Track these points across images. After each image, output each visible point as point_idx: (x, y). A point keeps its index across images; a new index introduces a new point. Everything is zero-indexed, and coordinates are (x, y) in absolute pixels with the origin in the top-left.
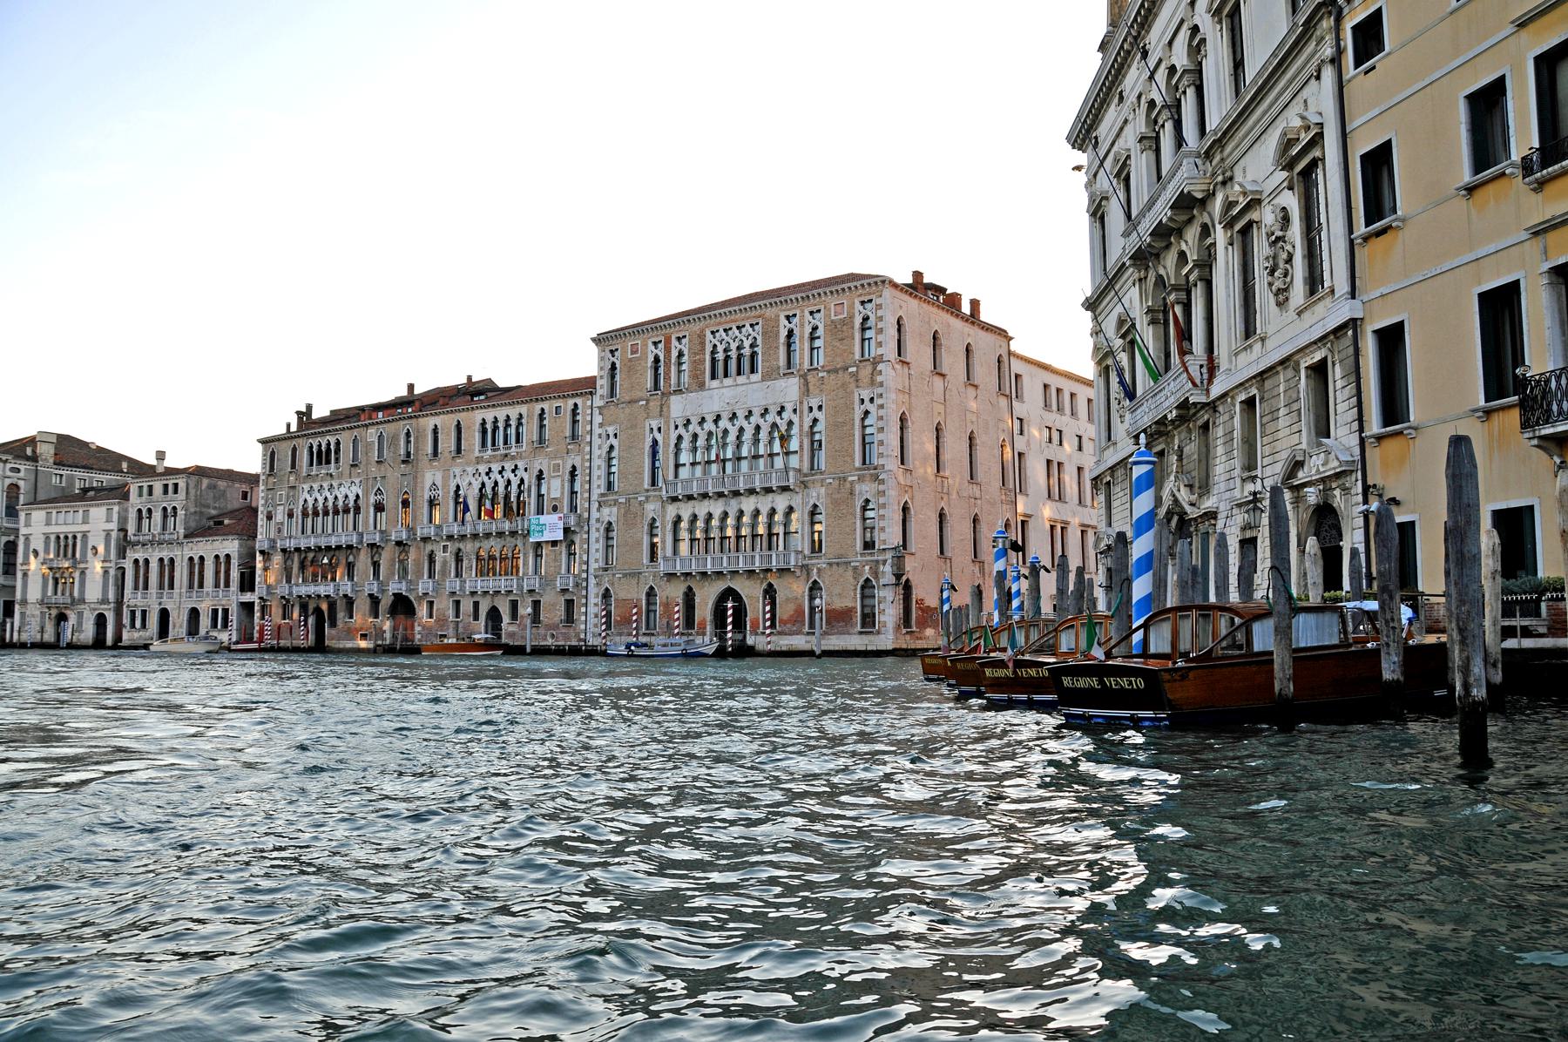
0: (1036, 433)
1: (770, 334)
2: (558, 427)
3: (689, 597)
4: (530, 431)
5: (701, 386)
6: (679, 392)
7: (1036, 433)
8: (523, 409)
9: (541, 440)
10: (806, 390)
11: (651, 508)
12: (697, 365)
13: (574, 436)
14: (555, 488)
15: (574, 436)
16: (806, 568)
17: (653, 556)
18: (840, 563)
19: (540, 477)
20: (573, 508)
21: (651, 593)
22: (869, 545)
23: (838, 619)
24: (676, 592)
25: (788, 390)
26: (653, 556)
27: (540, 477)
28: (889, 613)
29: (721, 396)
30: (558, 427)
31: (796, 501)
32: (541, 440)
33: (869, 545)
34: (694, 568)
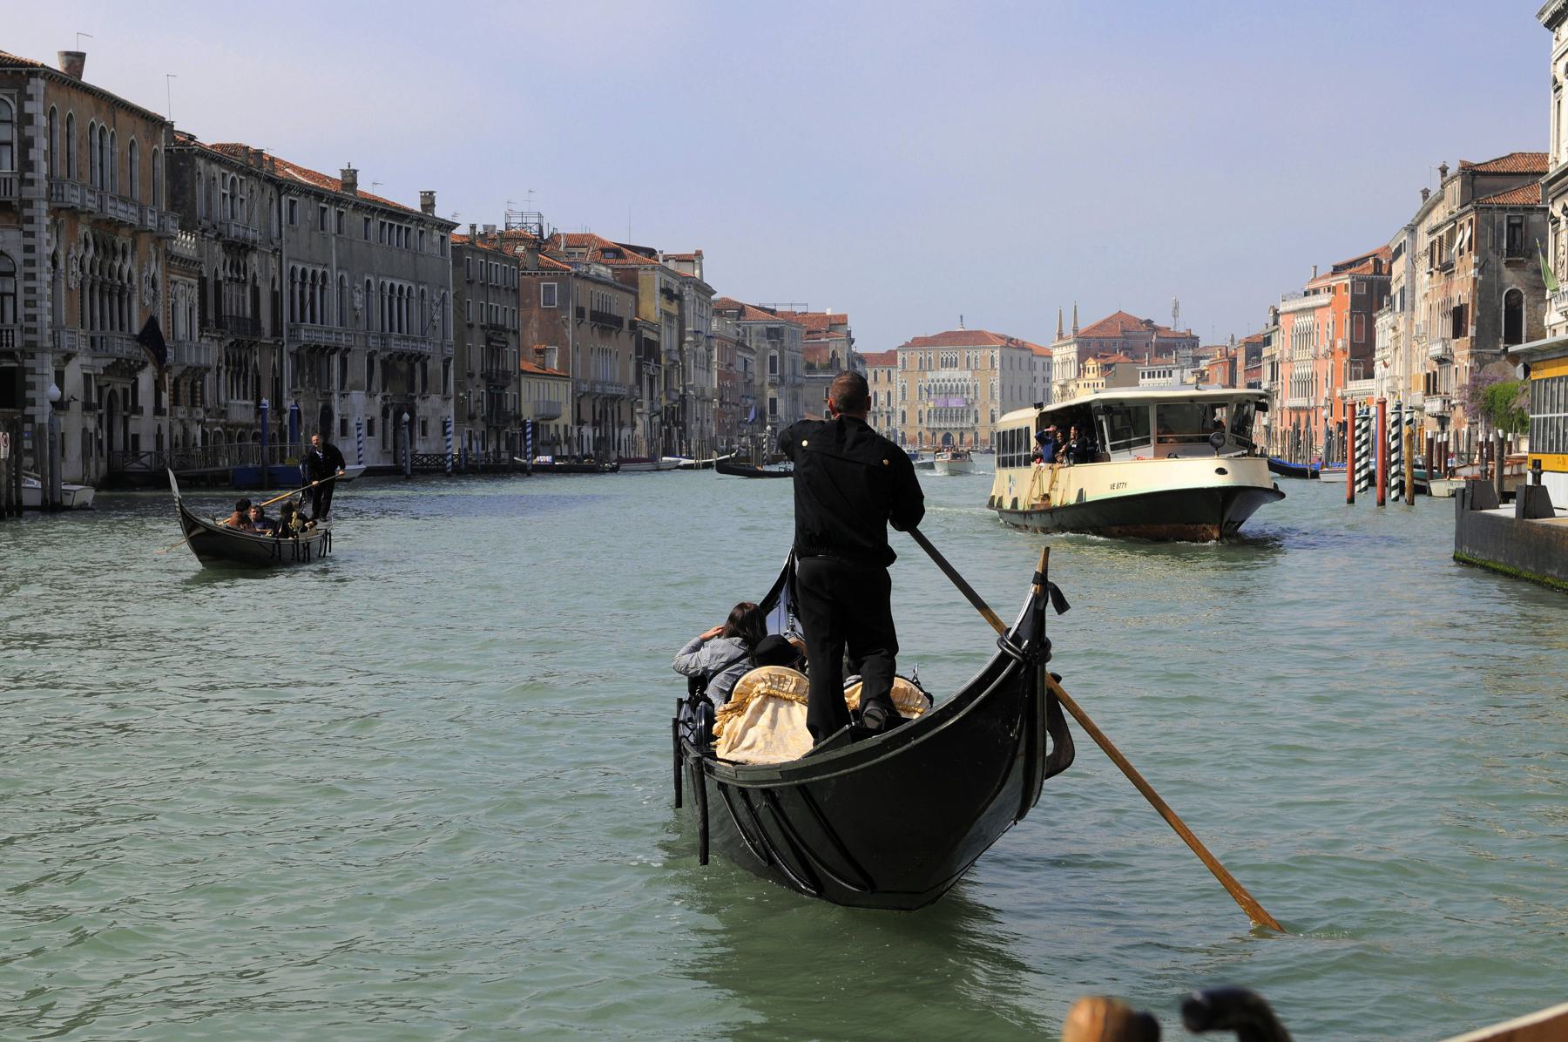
0: (1039, 380)
7: (1039, 380)
25: (969, 374)
29: (945, 373)
30: (882, 376)
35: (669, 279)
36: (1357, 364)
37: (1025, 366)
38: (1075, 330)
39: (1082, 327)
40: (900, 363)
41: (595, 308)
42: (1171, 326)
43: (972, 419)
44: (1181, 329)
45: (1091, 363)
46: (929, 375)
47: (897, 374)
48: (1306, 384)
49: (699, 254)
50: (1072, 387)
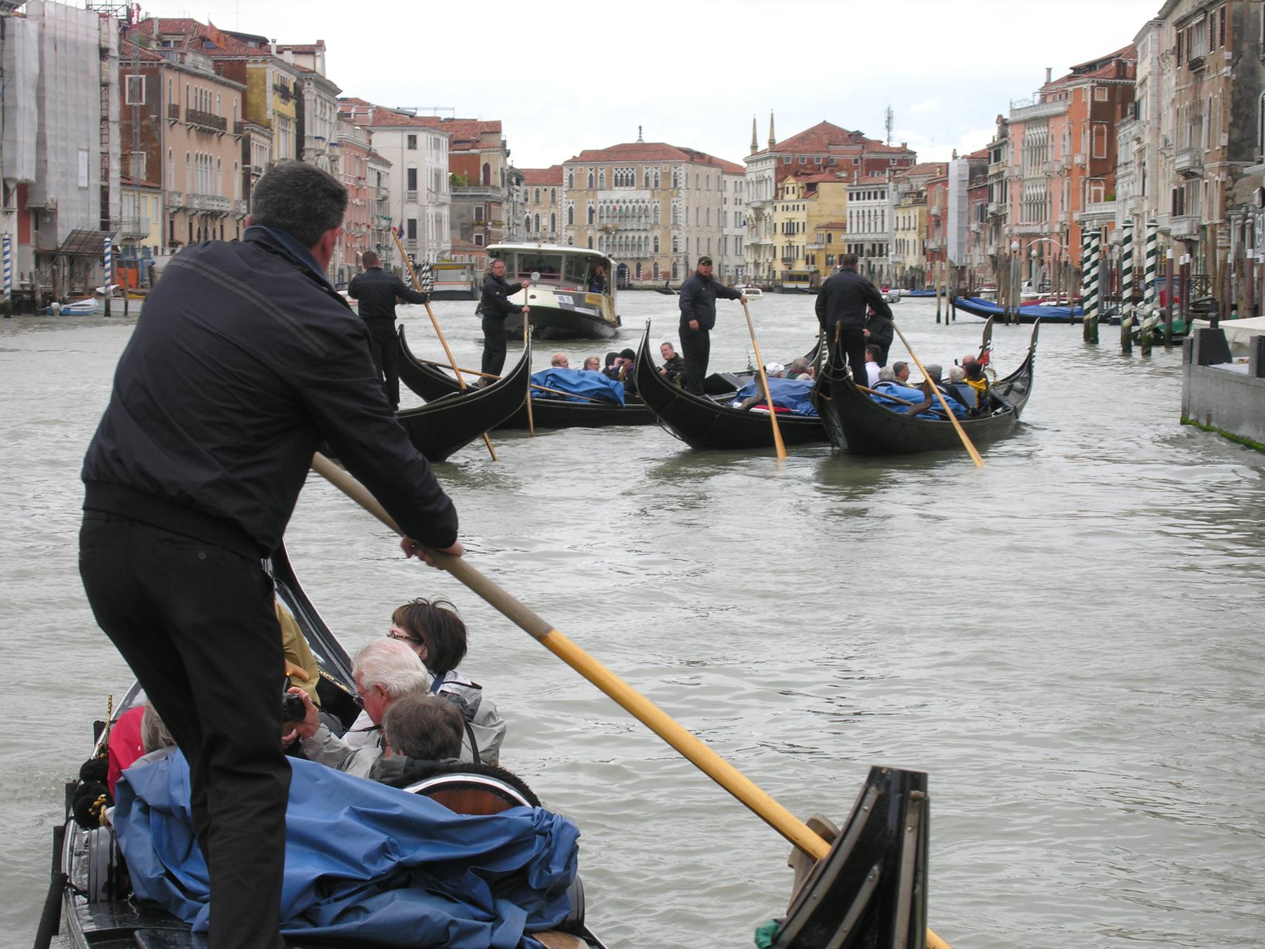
0: (730, 202)
1: (639, 173)
2: (546, 197)
4: (532, 197)
7: (730, 202)
8: (528, 188)
9: (537, 201)
11: (590, 233)
13: (553, 201)
14: (545, 221)
15: (553, 201)
16: (653, 258)
18: (665, 256)
19: (537, 216)
20: (553, 230)
22: (675, 250)
23: (666, 275)
25: (646, 195)
27: (537, 216)
29: (620, 193)
30: (546, 197)
31: (649, 234)
32: (537, 201)
33: (675, 250)
35: (284, 74)
36: (1097, 183)
37: (713, 184)
38: (772, 142)
39: (779, 139)
40: (566, 181)
41: (192, 107)
43: (651, 248)
44: (896, 144)
45: (791, 182)
46: (601, 195)
47: (562, 193)
48: (1039, 206)
49: (320, 44)
50: (768, 210)
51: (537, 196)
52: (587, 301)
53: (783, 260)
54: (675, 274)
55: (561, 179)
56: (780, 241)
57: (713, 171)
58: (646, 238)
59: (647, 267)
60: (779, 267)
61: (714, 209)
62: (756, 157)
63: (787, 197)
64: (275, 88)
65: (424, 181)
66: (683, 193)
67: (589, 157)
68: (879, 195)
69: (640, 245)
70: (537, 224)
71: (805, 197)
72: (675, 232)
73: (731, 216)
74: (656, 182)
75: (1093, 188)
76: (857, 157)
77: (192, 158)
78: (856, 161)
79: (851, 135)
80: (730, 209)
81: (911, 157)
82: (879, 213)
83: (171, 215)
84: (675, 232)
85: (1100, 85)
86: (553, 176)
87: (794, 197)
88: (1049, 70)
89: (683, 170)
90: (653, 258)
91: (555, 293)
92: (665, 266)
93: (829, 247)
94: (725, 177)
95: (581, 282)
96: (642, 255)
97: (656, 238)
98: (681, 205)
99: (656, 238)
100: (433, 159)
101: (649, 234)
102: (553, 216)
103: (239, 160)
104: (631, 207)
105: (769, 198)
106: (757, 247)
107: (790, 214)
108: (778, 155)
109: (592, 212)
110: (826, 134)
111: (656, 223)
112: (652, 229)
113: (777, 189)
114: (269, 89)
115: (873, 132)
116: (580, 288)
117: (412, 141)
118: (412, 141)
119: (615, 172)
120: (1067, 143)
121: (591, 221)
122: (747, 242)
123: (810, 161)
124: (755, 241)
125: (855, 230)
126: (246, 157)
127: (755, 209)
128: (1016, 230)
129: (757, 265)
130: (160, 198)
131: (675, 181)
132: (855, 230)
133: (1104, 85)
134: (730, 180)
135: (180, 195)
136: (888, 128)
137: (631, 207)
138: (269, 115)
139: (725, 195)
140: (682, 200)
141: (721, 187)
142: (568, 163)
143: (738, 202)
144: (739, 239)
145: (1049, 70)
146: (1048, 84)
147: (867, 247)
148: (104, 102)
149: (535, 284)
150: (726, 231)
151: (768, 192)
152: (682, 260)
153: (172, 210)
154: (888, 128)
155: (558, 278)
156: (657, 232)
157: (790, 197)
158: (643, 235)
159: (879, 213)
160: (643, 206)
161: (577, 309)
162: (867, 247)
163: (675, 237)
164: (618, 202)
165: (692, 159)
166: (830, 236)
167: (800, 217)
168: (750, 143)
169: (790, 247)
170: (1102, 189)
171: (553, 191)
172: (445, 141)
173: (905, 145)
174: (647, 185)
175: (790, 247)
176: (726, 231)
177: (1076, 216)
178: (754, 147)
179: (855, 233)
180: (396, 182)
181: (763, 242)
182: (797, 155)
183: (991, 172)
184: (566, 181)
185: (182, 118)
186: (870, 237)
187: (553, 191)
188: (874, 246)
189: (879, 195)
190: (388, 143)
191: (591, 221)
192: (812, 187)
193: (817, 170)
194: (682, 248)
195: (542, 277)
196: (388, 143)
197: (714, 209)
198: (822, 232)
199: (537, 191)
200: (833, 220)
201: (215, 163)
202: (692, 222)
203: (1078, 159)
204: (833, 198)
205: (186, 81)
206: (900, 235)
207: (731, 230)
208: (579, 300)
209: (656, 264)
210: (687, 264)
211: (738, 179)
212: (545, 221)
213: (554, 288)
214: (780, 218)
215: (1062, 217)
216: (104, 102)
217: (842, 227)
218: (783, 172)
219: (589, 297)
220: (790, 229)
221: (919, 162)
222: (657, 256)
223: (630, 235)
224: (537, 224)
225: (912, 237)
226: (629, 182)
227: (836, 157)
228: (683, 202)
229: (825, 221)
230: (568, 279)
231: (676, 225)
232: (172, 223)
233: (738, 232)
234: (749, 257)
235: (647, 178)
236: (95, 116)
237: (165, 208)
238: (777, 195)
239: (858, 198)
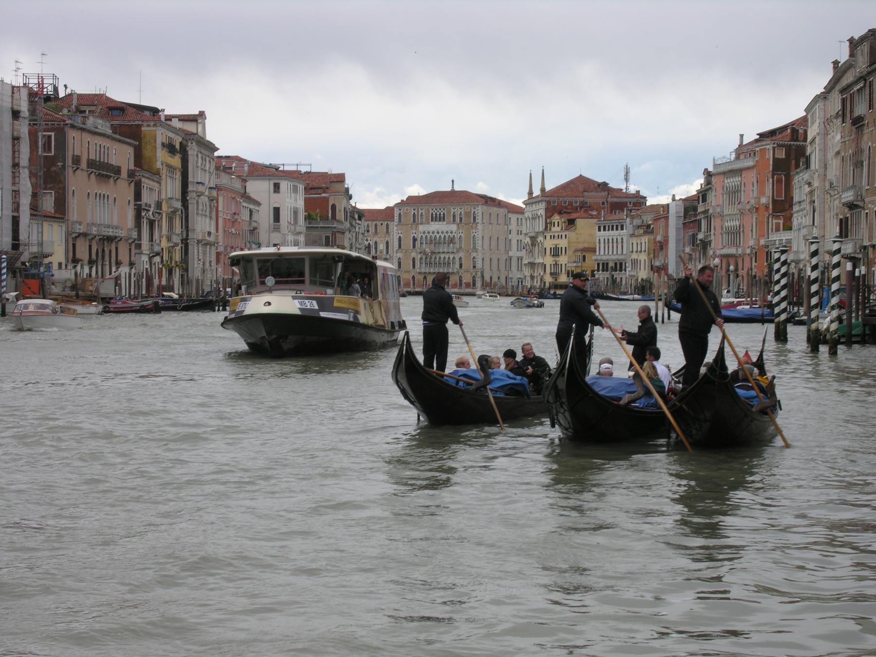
0: (514, 233)
1: (449, 212)
2: (382, 229)
3: (425, 278)
4: (372, 229)
5: (428, 223)
6: (422, 224)
7: (514, 233)
8: (370, 223)
10: (458, 228)
11: (413, 255)
12: (427, 217)
13: (387, 232)
14: (382, 247)
15: (387, 232)
16: (458, 272)
17: (414, 266)
19: (376, 243)
21: (413, 277)
22: (474, 267)
23: (468, 285)
24: (421, 277)
25: (454, 227)
26: (414, 266)
27: (376, 243)
28: (479, 284)
29: (435, 226)
30: (382, 229)
31: (456, 256)
33: (474, 267)
34: (427, 271)
35: (171, 135)
36: (777, 217)
37: (501, 220)
38: (543, 190)
39: (548, 188)
40: (396, 218)
41: (92, 157)
42: (623, 187)
43: (457, 266)
44: (632, 189)
45: (556, 218)
46: (421, 228)
47: (394, 226)
48: (735, 235)
49: (202, 114)
50: (540, 239)
51: (376, 228)
52: (336, 304)
53: (551, 274)
54: (474, 284)
55: (393, 217)
56: (549, 260)
57: (502, 211)
58: (454, 258)
59: (453, 279)
60: (548, 279)
61: (502, 238)
62: (531, 200)
63: (553, 229)
64: (163, 145)
65: (285, 216)
66: (480, 227)
67: (412, 201)
68: (619, 228)
69: (449, 264)
70: (376, 248)
71: (567, 229)
72: (474, 254)
73: (514, 243)
74: (461, 219)
75: (774, 221)
76: (604, 200)
77: (92, 196)
78: (603, 203)
79: (599, 185)
80: (514, 237)
81: (642, 200)
82: (620, 240)
83: (73, 240)
84: (474, 254)
85: (779, 145)
86: (387, 214)
87: (559, 229)
88: (742, 136)
89: (480, 210)
90: (458, 272)
91: (294, 298)
92: (467, 278)
93: (584, 264)
94: (510, 215)
95: (330, 285)
96: (450, 271)
97: (460, 258)
98: (479, 235)
99: (460, 258)
100: (292, 200)
101: (456, 256)
102: (387, 243)
103: (131, 197)
104: (442, 236)
105: (541, 230)
106: (532, 265)
107: (556, 241)
108: (547, 199)
109: (415, 240)
110: (581, 184)
111: (461, 248)
112: (458, 251)
113: (546, 223)
114: (159, 145)
115: (616, 183)
116: (330, 292)
117: (277, 188)
118: (277, 188)
119: (431, 211)
120: (755, 188)
121: (414, 246)
122: (525, 261)
123: (571, 203)
124: (531, 260)
125: (602, 253)
126: (138, 196)
127: (531, 238)
128: (718, 252)
129: (532, 277)
130: (64, 225)
131: (474, 218)
132: (602, 253)
133: (782, 146)
134: (514, 217)
135: (80, 223)
136: (627, 180)
137: (442, 236)
138: (159, 165)
139: (510, 228)
140: (479, 231)
141: (507, 222)
142: (397, 205)
143: (519, 233)
144: (520, 259)
145: (742, 136)
146: (741, 146)
147: (611, 264)
148: (15, 152)
149: (270, 290)
150: (511, 254)
151: (540, 226)
152: (479, 274)
153: (74, 235)
154: (627, 180)
155: (303, 282)
156: (461, 254)
157: (556, 229)
158: (451, 257)
159: (620, 240)
160: (451, 235)
161: (323, 314)
162: (611, 264)
163: (474, 258)
164: (433, 232)
165: (486, 202)
166: (584, 257)
167: (563, 243)
168: (527, 190)
169: (556, 264)
170: (781, 222)
171: (387, 225)
172: (301, 187)
173: (638, 192)
174: (454, 220)
175: (556, 264)
176: (511, 254)
177: (762, 242)
178: (530, 193)
179: (602, 255)
180: (264, 217)
181: (537, 261)
182: (561, 199)
183: (700, 210)
184: (396, 218)
185: (84, 164)
186: (613, 257)
187: (387, 225)
188: (616, 264)
189: (619, 228)
190: (258, 188)
191: (414, 246)
192: (571, 222)
193: (575, 210)
194: (479, 265)
195: (277, 283)
196: (258, 188)
197: (502, 238)
198: (579, 254)
199: (376, 225)
200: (586, 245)
201: (111, 200)
202: (486, 247)
203: (764, 200)
204: (587, 230)
205: (87, 137)
206: (634, 256)
207: (514, 253)
208: (324, 304)
209: (460, 277)
210: (483, 277)
211: (520, 216)
212: (382, 247)
213: (293, 293)
214: (549, 244)
215: (752, 243)
216: (15, 152)
217: (593, 250)
218: (551, 211)
219: (340, 300)
220: (556, 252)
221: (648, 204)
222: (461, 271)
223: (442, 256)
224: (376, 248)
225: (643, 257)
226: (441, 218)
227: (588, 200)
228: (480, 233)
229: (581, 246)
230: (313, 282)
231: (475, 249)
232: (74, 245)
233: (519, 254)
234: (527, 272)
235: (454, 216)
236: (7, 162)
237: (68, 234)
238: (546, 227)
239: (604, 230)
